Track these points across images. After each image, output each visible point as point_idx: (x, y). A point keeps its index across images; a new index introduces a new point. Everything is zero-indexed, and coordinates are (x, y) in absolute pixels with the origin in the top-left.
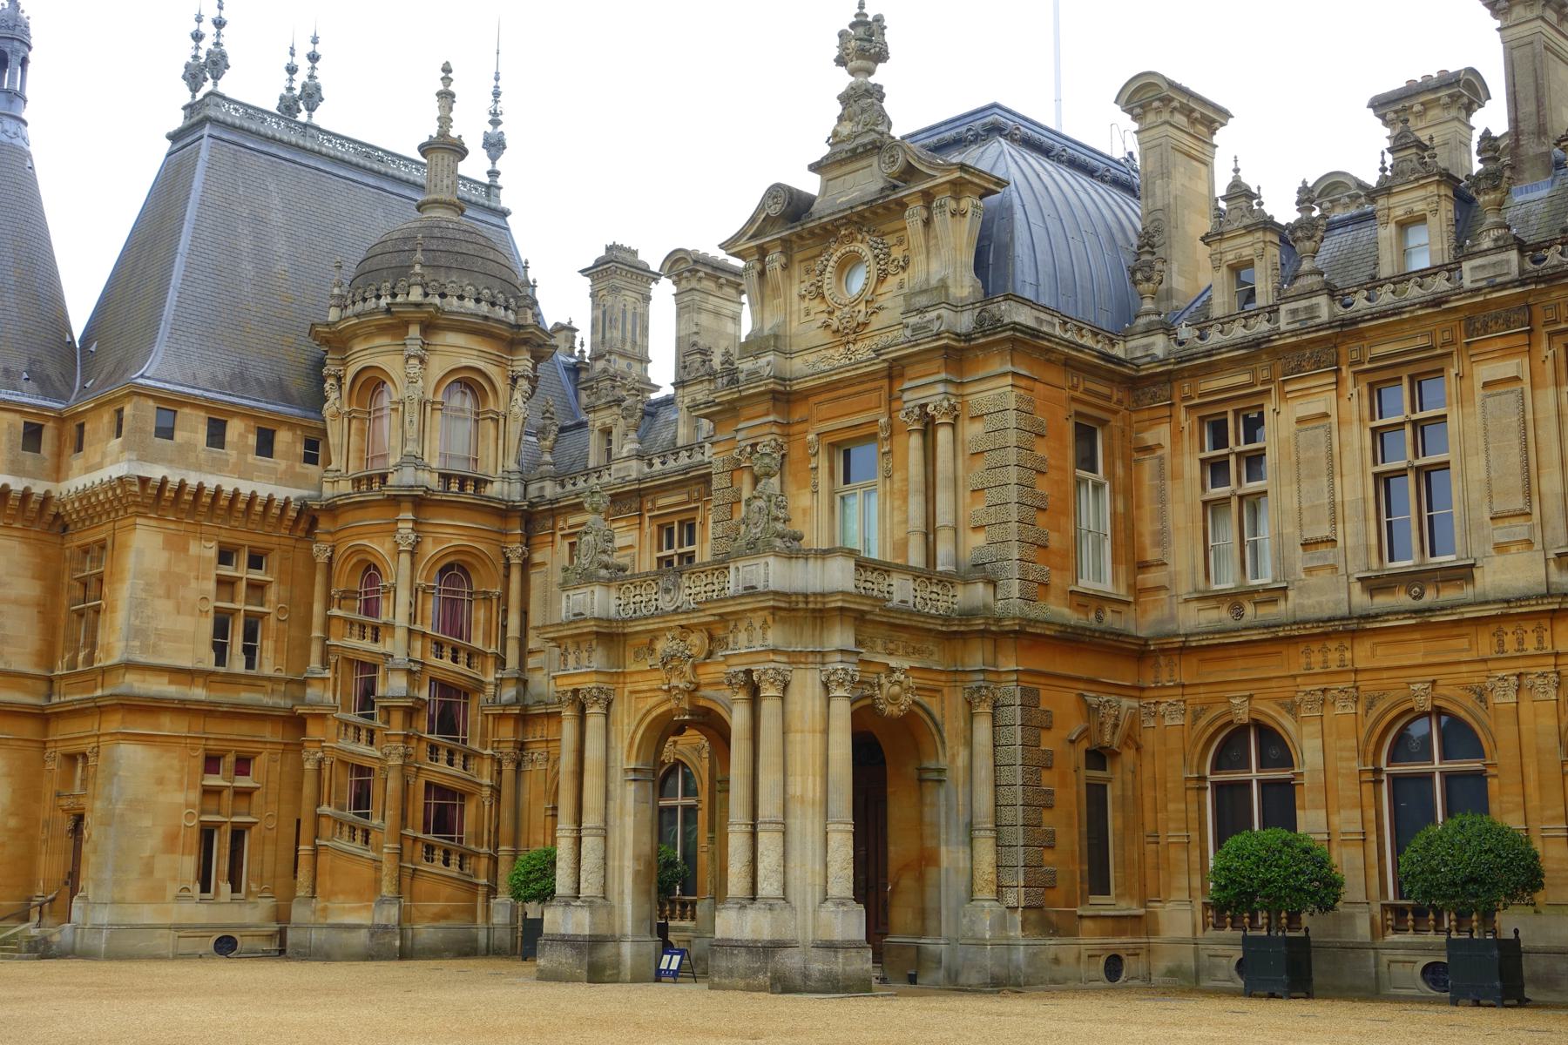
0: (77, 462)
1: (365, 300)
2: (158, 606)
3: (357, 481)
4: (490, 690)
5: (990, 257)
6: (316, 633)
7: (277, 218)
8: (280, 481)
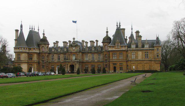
0: (30, 50)
2: (35, 58)
5: (80, 48)
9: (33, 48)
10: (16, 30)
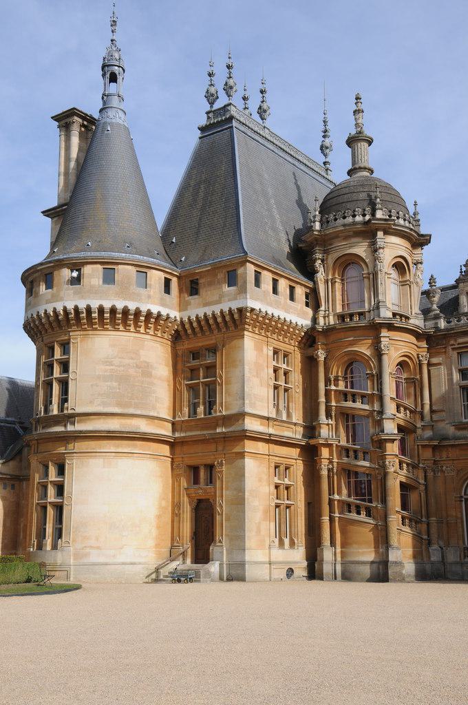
0: (194, 300)
1: (344, 218)
3: (342, 317)
4: (419, 431)
6: (322, 399)
7: (266, 176)
8: (299, 315)
9: (216, 268)
10: (56, 118)
